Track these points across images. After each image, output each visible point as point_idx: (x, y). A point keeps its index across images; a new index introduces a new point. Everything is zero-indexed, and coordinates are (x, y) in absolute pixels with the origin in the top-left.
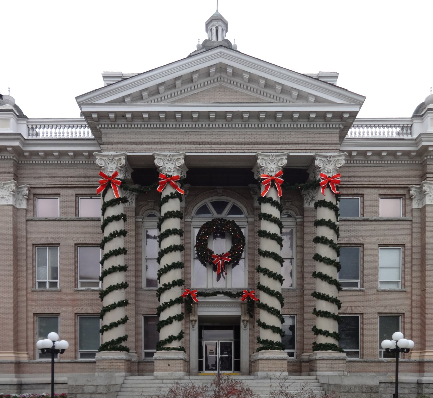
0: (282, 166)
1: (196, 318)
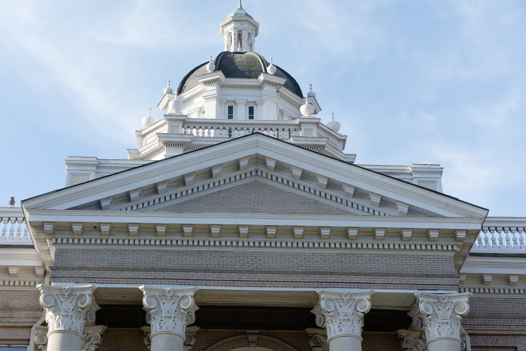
0: (362, 311)
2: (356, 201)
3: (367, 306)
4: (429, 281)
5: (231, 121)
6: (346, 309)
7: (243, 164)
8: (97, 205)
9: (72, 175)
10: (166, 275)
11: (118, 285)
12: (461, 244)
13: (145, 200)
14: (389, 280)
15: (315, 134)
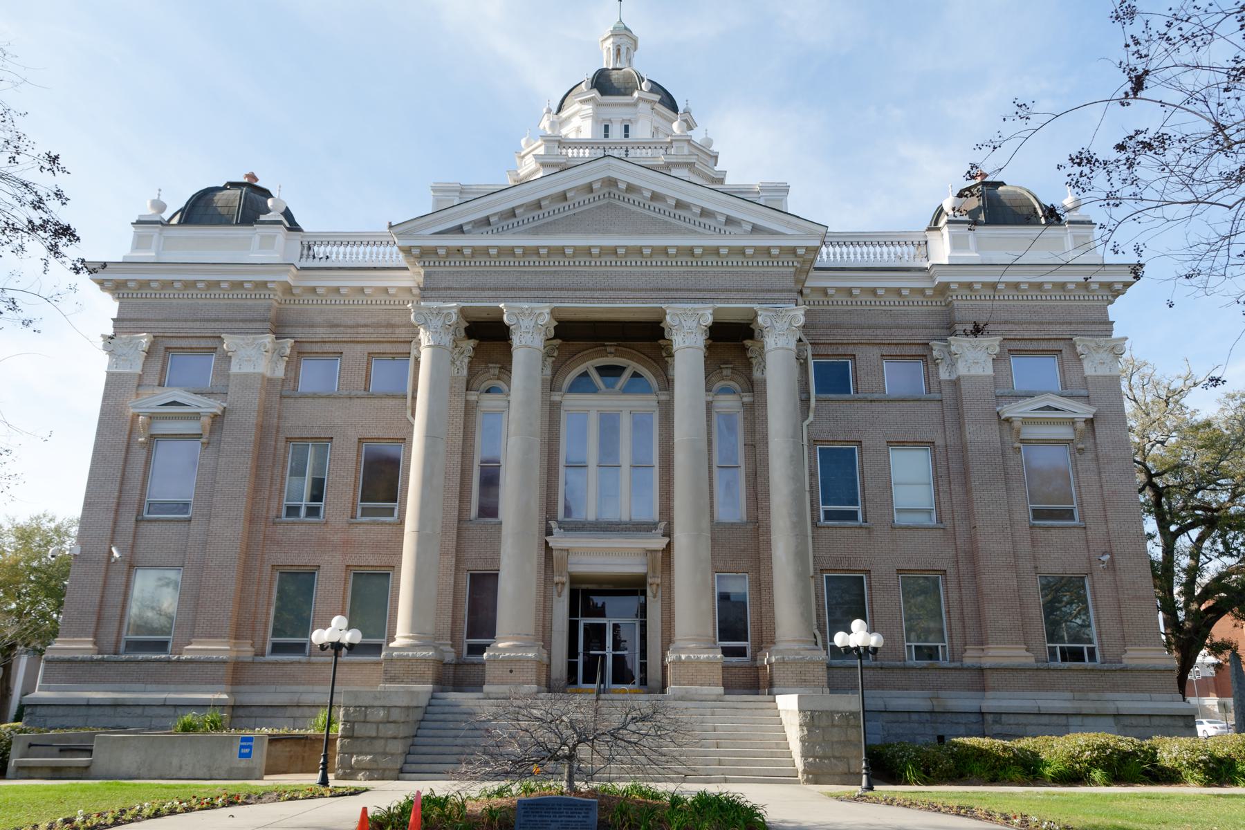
1: (565, 579)
2: (703, 220)
3: (709, 320)
4: (768, 295)
5: (606, 140)
6: (690, 323)
7: (595, 186)
8: (459, 230)
9: (437, 201)
10: (525, 294)
11: (481, 304)
12: (804, 261)
13: (504, 223)
14: (732, 295)
15: (686, 152)
